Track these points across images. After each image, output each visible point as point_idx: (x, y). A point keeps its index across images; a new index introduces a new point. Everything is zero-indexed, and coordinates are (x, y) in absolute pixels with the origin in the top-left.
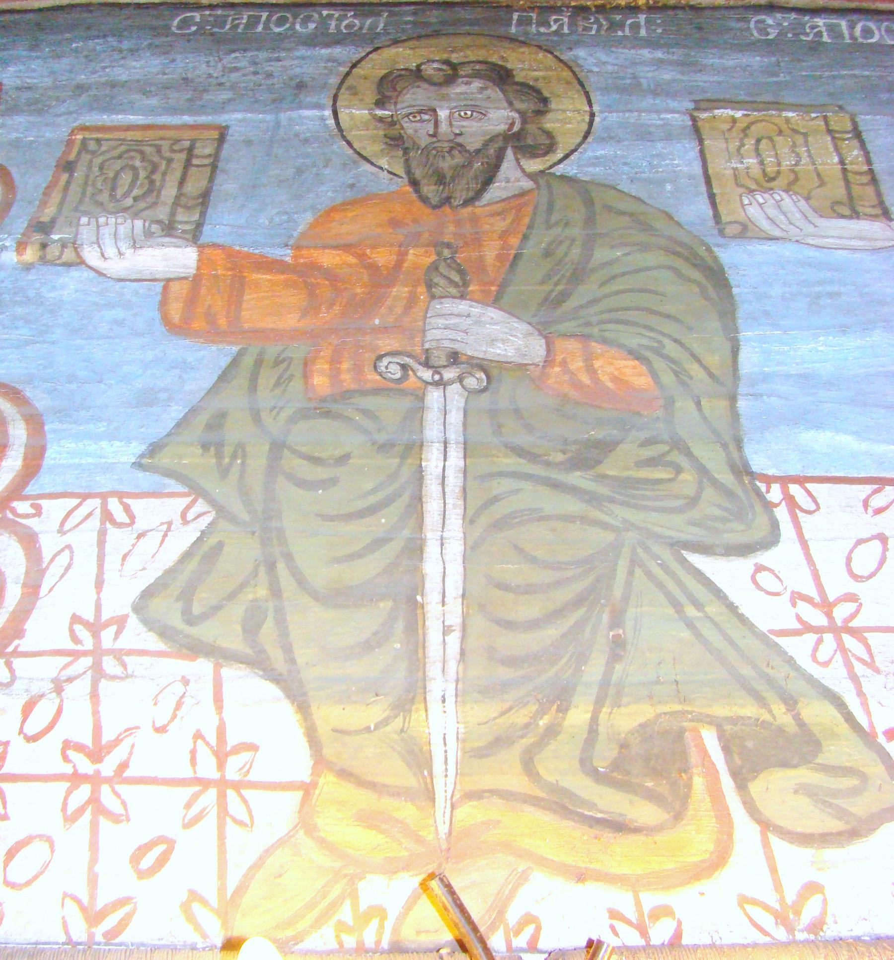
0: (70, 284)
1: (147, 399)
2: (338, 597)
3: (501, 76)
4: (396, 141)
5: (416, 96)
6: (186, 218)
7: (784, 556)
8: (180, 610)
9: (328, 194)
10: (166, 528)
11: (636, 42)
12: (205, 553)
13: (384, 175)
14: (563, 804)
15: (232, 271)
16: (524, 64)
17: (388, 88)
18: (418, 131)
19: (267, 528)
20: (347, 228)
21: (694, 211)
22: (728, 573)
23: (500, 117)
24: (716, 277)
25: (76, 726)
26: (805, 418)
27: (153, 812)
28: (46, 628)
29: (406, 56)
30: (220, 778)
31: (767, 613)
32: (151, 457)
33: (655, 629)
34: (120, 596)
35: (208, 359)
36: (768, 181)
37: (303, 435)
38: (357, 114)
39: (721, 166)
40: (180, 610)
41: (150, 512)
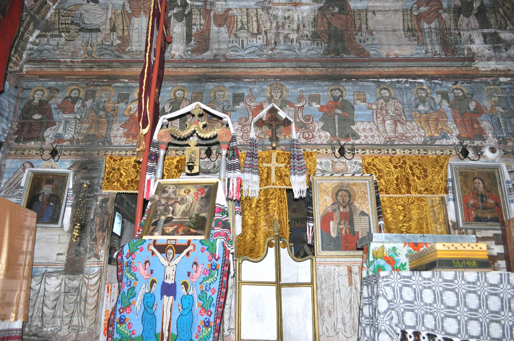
0: (312, 107)
1: (319, 116)
2: (331, 128)
3: (339, 90)
4: (332, 96)
5: (333, 92)
6: (318, 103)
7: (355, 126)
8: (323, 128)
9: (328, 101)
10: (321, 124)
11: (350, 86)
12: (324, 125)
13: (331, 99)
14: (343, 138)
15: (322, 107)
16: (341, 88)
17: (331, 90)
18: (334, 95)
19: (327, 124)
20: (329, 104)
21: (352, 102)
22: (352, 127)
23: (340, 94)
24: (353, 108)
25: (319, 134)
26: (358, 118)
27: (323, 138)
28: (316, 129)
29: (332, 88)
30: (326, 137)
31: (354, 129)
32: (320, 120)
33: (348, 129)
34: (320, 128)
35: (322, 113)
36: (358, 99)
37: (329, 118)
38: (329, 93)
39: (355, 98)
40: (323, 128)
41: (320, 123)
